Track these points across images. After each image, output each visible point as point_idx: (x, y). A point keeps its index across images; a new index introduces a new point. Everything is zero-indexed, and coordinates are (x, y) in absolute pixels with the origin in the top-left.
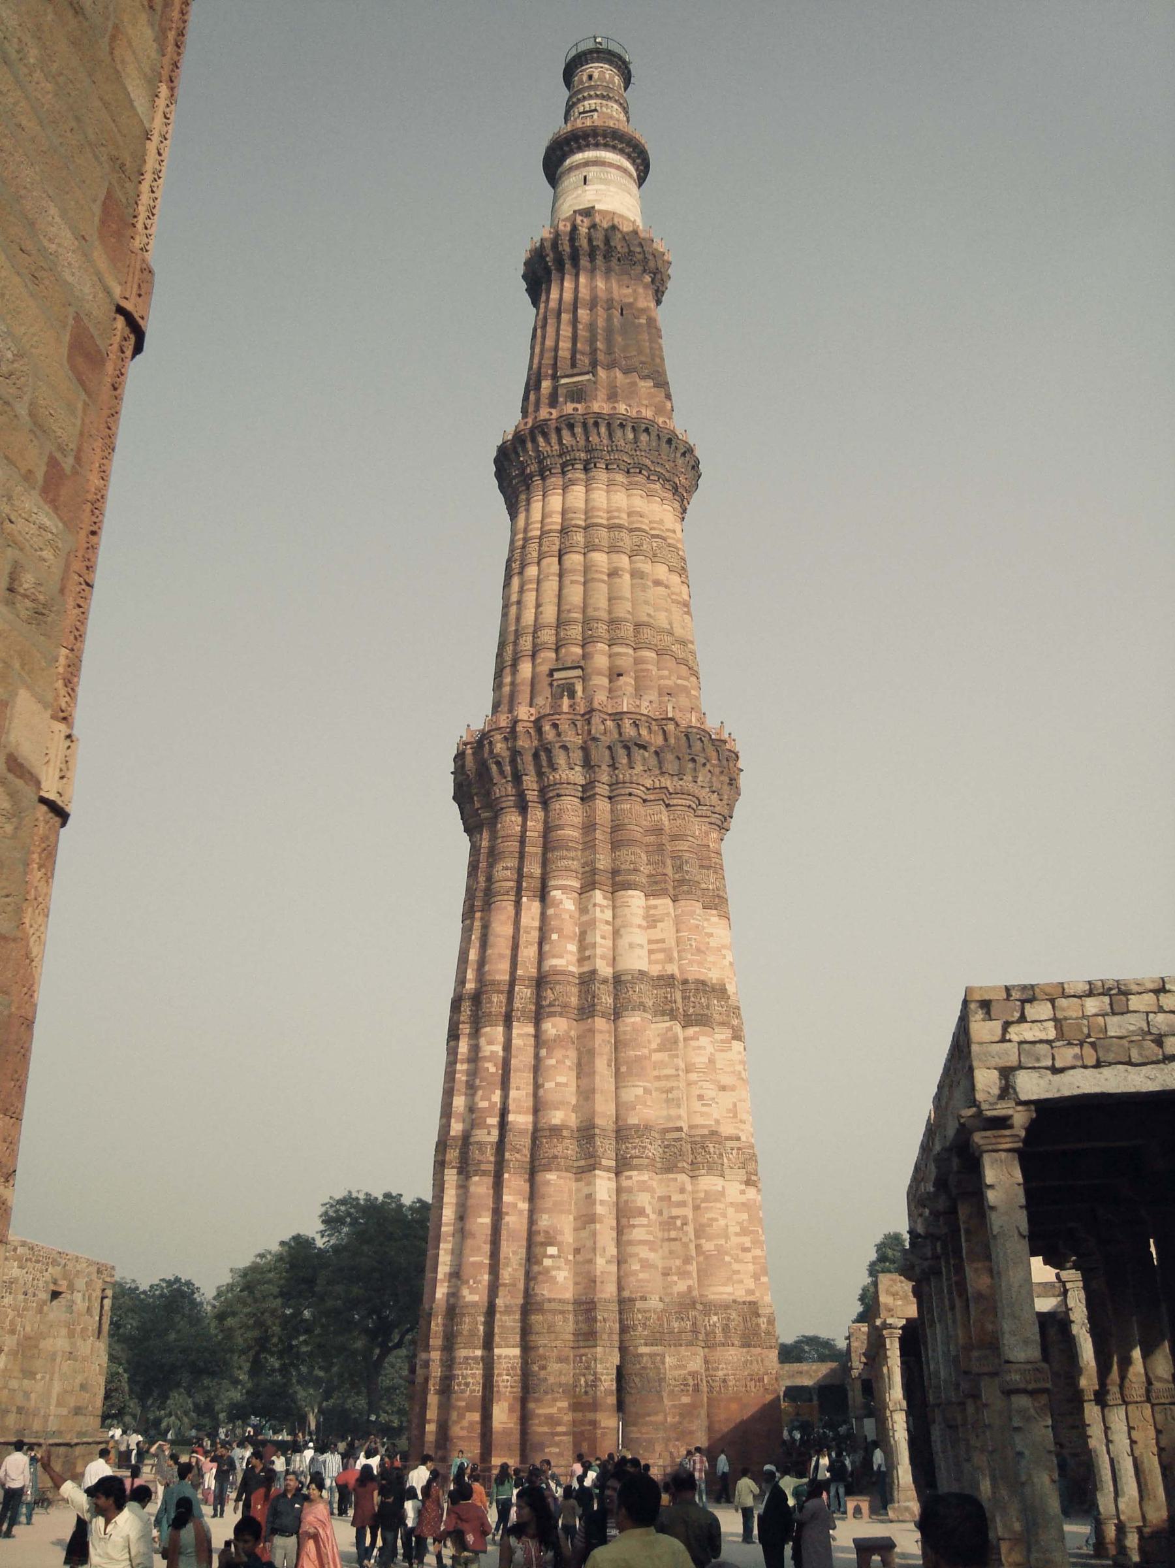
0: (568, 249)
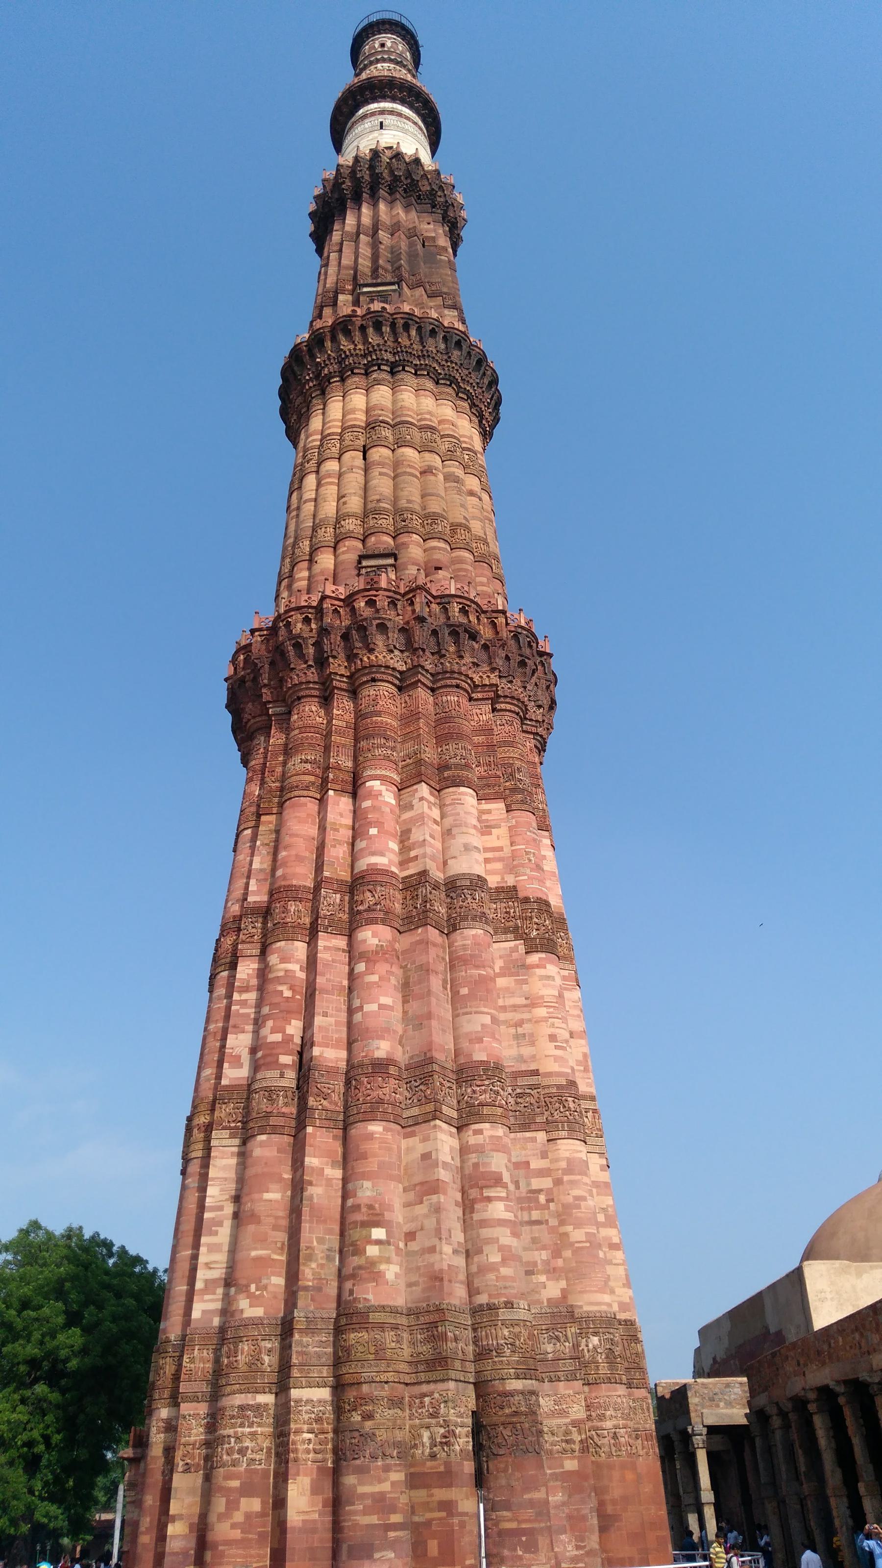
0: (367, 178)
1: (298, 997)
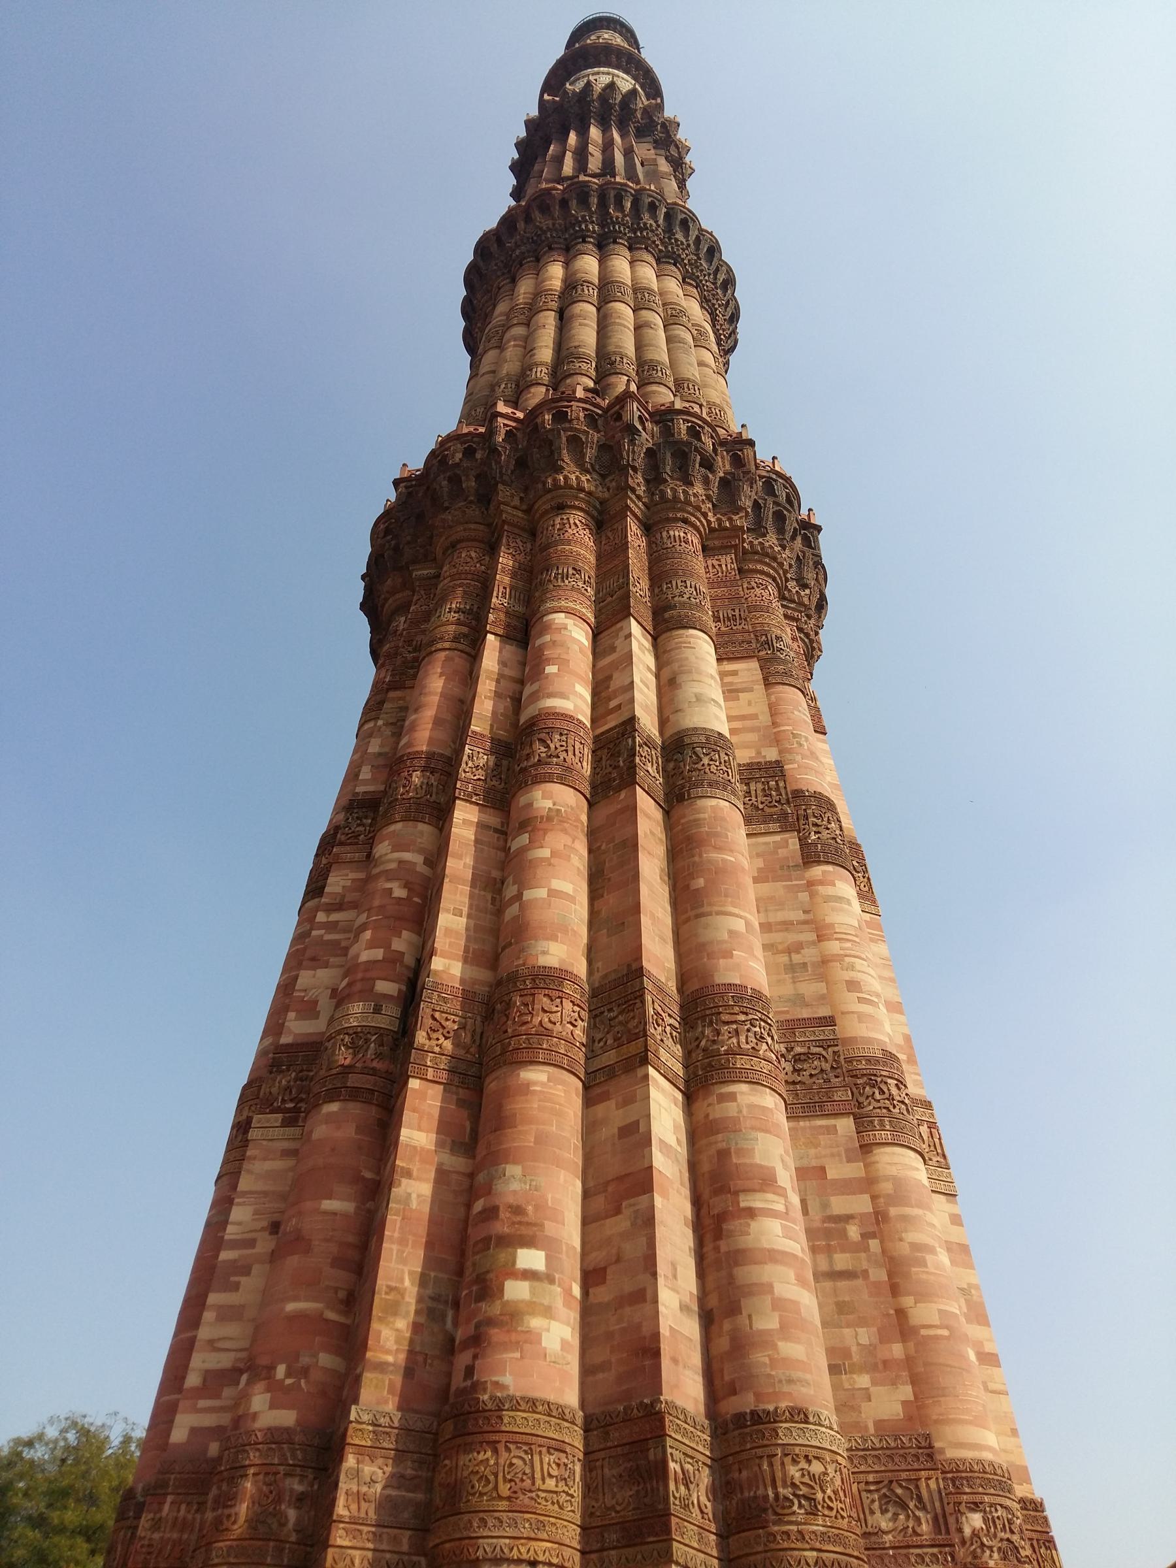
1: (416, 899)
